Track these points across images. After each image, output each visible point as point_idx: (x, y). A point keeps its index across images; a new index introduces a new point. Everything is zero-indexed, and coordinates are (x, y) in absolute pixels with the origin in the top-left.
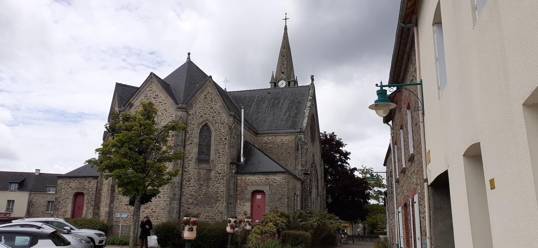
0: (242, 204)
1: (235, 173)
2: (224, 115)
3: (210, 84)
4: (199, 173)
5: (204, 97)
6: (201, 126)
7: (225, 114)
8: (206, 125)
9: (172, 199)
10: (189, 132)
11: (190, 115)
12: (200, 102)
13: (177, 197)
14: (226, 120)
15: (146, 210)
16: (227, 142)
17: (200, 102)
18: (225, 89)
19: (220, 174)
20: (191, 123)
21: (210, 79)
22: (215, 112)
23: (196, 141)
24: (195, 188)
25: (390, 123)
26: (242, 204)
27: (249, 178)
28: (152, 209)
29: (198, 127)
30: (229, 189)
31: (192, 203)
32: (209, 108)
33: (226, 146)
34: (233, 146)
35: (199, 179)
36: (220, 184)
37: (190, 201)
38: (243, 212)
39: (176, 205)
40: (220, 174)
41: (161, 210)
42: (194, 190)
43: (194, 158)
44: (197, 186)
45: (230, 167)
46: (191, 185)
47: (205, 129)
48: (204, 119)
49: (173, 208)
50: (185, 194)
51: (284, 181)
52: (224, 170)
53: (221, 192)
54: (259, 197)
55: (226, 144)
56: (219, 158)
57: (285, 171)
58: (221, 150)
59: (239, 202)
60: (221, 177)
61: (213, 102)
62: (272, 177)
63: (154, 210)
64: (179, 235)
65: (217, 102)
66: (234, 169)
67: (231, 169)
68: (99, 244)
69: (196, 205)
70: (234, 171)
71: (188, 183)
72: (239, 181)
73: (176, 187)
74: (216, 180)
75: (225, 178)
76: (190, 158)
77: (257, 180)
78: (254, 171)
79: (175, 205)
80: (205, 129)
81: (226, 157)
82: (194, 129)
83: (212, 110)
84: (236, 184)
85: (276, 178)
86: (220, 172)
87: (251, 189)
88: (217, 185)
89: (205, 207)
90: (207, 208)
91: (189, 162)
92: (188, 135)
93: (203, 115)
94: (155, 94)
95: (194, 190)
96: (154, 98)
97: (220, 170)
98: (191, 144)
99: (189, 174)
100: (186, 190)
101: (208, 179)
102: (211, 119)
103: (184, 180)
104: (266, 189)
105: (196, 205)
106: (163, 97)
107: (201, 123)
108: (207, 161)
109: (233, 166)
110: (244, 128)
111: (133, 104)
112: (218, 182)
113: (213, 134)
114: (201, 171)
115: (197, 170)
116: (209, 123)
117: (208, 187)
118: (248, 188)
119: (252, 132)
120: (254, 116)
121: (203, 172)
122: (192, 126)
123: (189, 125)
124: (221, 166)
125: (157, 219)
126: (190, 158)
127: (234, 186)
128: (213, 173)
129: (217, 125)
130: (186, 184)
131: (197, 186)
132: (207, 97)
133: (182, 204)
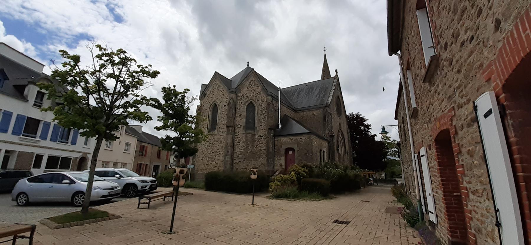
0: (279, 158)
1: (273, 136)
2: (264, 95)
3: (253, 74)
4: (246, 136)
5: (249, 83)
6: (247, 104)
7: (264, 94)
8: (251, 102)
9: (226, 155)
10: (239, 108)
11: (239, 96)
12: (246, 87)
13: (230, 153)
14: (265, 99)
15: (213, 163)
16: (266, 114)
17: (246, 87)
18: (280, 87)
19: (262, 137)
20: (240, 102)
21: (253, 71)
22: (257, 93)
23: (244, 114)
24: (244, 147)
25: (399, 52)
26: (279, 158)
27: (283, 139)
28: (216, 162)
29: (245, 104)
30: (268, 148)
31: (241, 158)
32: (253, 91)
33: (266, 117)
34: (271, 116)
35: (246, 141)
36: (262, 144)
37: (240, 156)
38: (279, 164)
39: (229, 159)
40: (262, 137)
41: (221, 163)
42: (243, 149)
43: (242, 126)
44: (245, 146)
45: (269, 132)
46: (241, 145)
47: (251, 106)
48: (249, 98)
49: (227, 161)
50: (236, 151)
51: (308, 140)
52: (265, 134)
53: (263, 149)
54: (291, 153)
55: (266, 115)
56: (261, 125)
57: (308, 132)
58: (262, 120)
59: (276, 157)
60: (263, 139)
61: (256, 87)
62: (299, 137)
63: (217, 163)
64: (250, 178)
65: (258, 87)
66: (272, 133)
67: (269, 133)
68: (141, 188)
69: (245, 159)
70: (272, 135)
71: (238, 143)
72: (276, 142)
73: (229, 146)
74: (259, 141)
75: (266, 140)
76: (239, 126)
77: (289, 141)
78: (286, 134)
79: (228, 158)
80: (251, 106)
81: (266, 125)
82: (242, 106)
83: (255, 92)
84: (274, 144)
85: (302, 138)
86: (262, 135)
87: (284, 147)
88: (260, 145)
89: (252, 161)
90: (253, 161)
91: (239, 129)
92: (237, 110)
93: (248, 96)
94: (218, 85)
95: (243, 149)
96: (217, 88)
97: (262, 134)
98: (240, 117)
99: (240, 137)
100: (237, 149)
101: (253, 141)
102: (254, 98)
103: (236, 142)
104: (296, 147)
105: (245, 159)
106: (222, 86)
107: (247, 102)
108: (253, 128)
109: (271, 131)
110: (281, 104)
111: (206, 94)
112: (261, 142)
113: (256, 108)
114: (248, 135)
115: (245, 134)
116: (253, 101)
117: (253, 146)
118: (283, 146)
119: (291, 109)
120: (296, 100)
121: (249, 136)
122: (240, 104)
123: (239, 103)
124: (263, 131)
125: (219, 169)
126: (239, 126)
127: (273, 145)
128: (257, 137)
129: (259, 102)
130: (237, 144)
131: (245, 146)
132: (251, 83)
133: (235, 159)
